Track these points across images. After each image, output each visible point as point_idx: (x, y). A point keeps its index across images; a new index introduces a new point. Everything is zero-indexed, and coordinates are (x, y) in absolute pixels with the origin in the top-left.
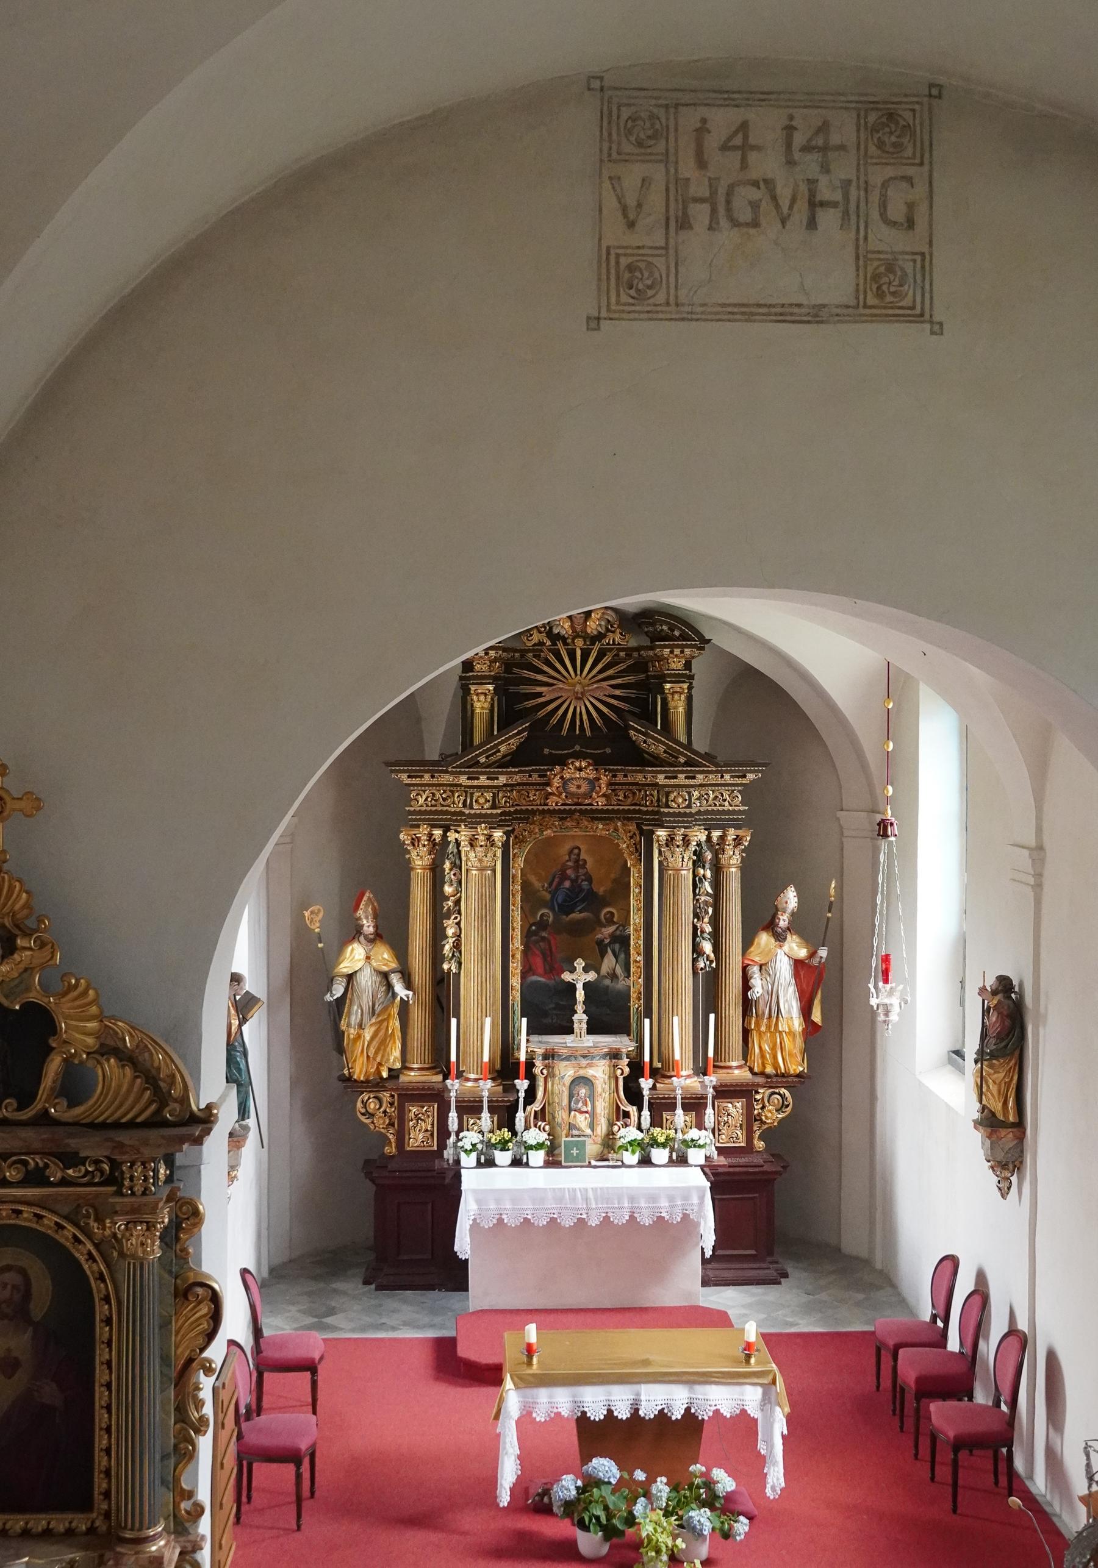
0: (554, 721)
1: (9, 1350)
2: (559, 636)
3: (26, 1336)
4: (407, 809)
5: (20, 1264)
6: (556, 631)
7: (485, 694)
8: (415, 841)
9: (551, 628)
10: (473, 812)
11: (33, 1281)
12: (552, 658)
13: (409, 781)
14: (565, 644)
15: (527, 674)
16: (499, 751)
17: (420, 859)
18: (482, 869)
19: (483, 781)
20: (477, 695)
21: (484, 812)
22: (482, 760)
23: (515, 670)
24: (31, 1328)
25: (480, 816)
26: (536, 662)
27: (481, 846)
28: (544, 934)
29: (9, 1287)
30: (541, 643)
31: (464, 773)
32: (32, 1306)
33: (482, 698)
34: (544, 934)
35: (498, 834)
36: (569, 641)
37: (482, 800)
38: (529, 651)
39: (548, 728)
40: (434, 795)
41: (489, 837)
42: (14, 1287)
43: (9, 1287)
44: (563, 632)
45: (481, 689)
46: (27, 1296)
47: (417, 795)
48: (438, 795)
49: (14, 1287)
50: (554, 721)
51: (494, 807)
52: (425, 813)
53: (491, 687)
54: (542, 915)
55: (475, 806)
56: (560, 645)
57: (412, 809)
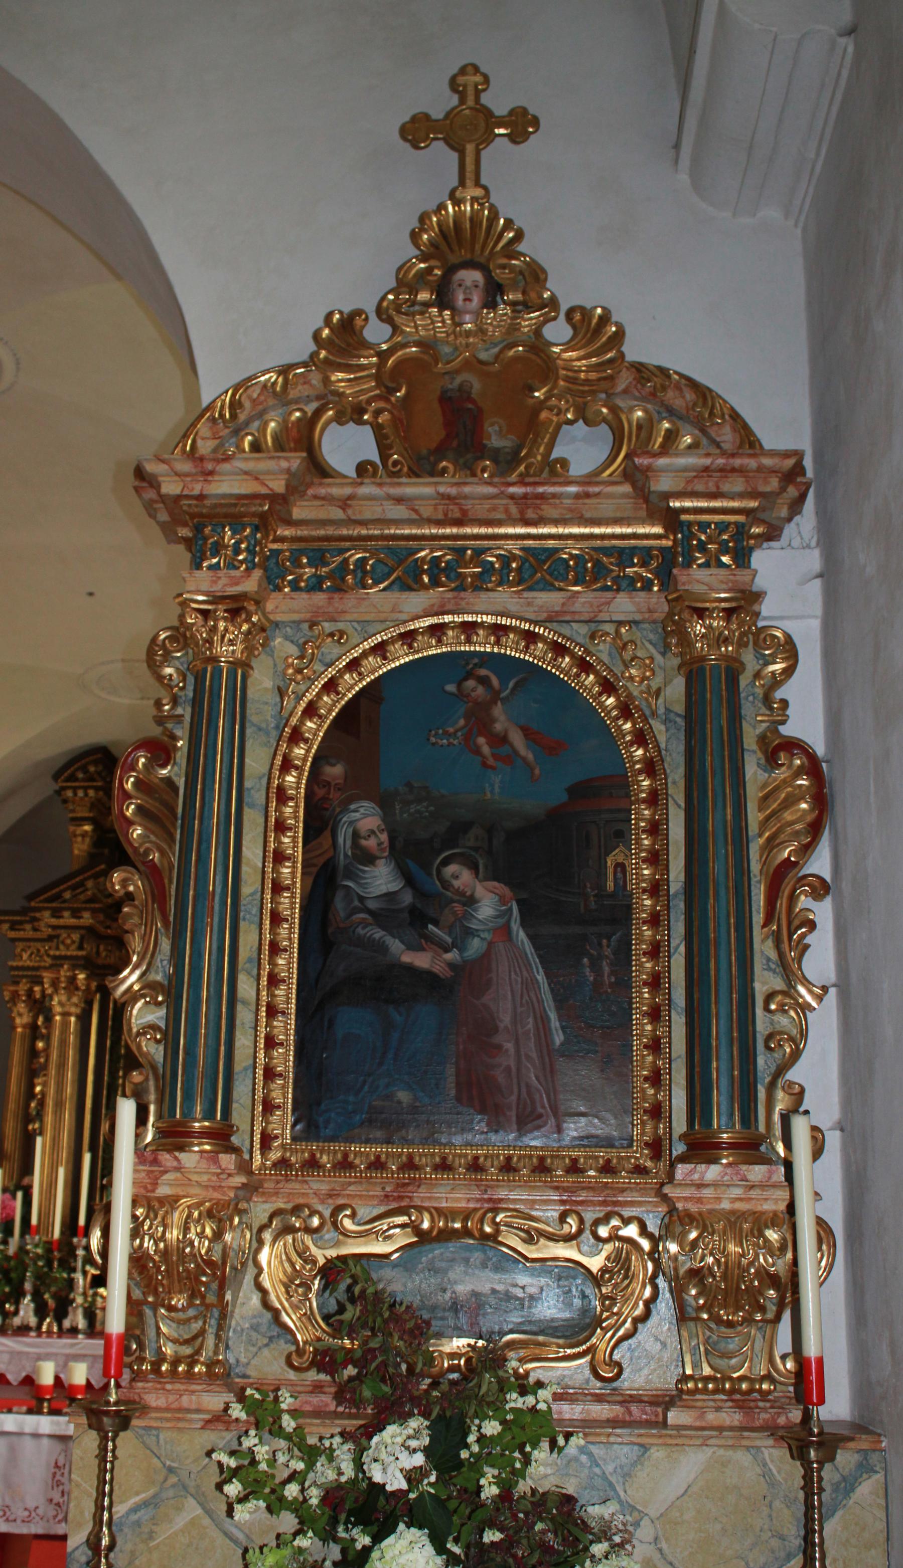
4: (10, 963)
8: (15, 996)
10: (57, 953)
13: (12, 934)
17: (22, 1017)
18: (65, 1015)
19: (67, 919)
21: (69, 953)
25: (66, 958)
33: (79, 839)
40: (38, 950)
41: (72, 980)
47: (23, 950)
48: (42, 951)
51: (81, 948)
52: (28, 968)
53: (87, 828)
55: (62, 947)
57: (15, 964)
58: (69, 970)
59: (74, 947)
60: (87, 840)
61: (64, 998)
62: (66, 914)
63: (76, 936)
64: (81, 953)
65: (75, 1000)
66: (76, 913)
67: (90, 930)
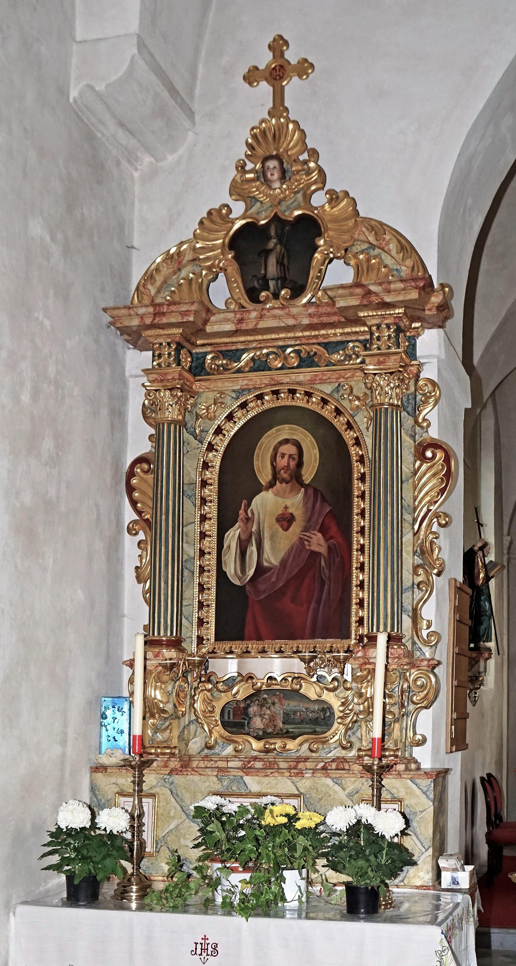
1: (286, 508)
3: (300, 495)
5: (295, 437)
24: (303, 489)
29: (286, 457)
42: (290, 456)
43: (286, 457)
46: (300, 464)
49: (290, 456)
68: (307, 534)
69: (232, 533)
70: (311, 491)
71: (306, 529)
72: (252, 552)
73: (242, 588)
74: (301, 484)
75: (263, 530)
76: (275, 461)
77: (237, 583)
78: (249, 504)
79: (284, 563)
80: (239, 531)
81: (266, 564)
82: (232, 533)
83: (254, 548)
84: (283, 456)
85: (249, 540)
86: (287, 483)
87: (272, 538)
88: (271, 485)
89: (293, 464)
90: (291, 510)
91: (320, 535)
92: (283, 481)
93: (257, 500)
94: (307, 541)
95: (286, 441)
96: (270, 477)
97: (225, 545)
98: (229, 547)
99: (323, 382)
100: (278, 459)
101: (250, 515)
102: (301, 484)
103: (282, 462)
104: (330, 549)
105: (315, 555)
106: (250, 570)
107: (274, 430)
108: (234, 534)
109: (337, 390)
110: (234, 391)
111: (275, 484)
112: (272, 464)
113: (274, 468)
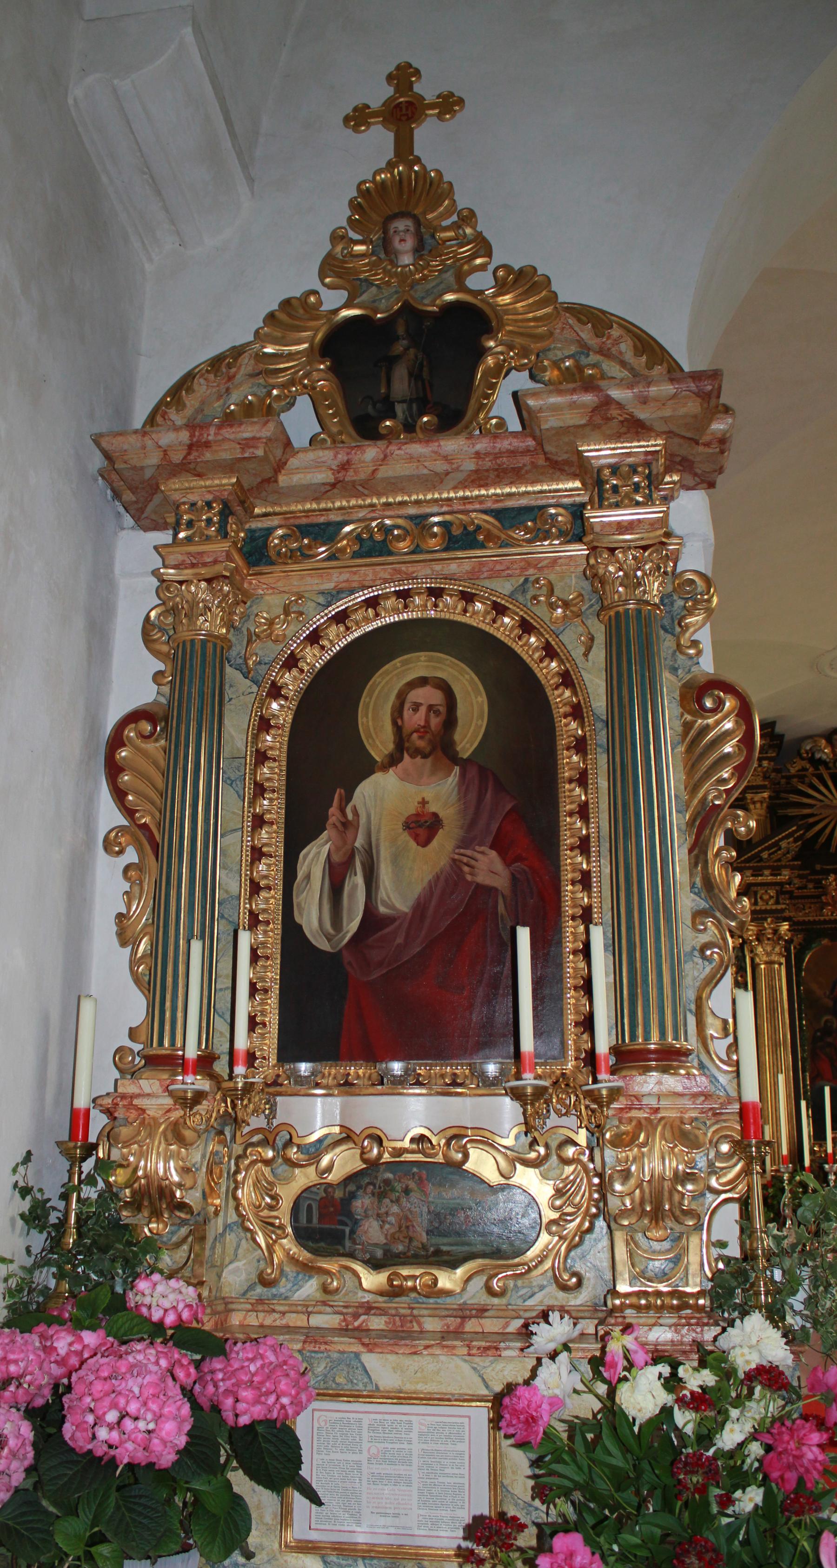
0: (822, 839)
1: (424, 802)
2: (821, 762)
3: (450, 779)
5: (439, 674)
6: (818, 756)
7: (761, 802)
9: (813, 754)
11: (458, 701)
12: (816, 782)
14: (827, 768)
15: (794, 798)
16: (780, 849)
18: (770, 963)
19: (767, 877)
20: (754, 803)
21: (768, 908)
22: (765, 855)
23: (783, 795)
24: (457, 769)
25: (766, 912)
26: (801, 787)
27: (769, 939)
28: (829, 1040)
30: (804, 769)
31: (749, 868)
32: (457, 737)
33: (758, 805)
34: (829, 1040)
35: (785, 927)
36: (831, 765)
37: (766, 897)
38: (794, 776)
39: (817, 847)
41: (775, 931)
42: (430, 708)
43: (423, 710)
44: (824, 757)
45: (757, 797)
46: (450, 722)
49: (430, 708)
50: (822, 839)
54: (826, 1021)
56: (822, 770)
58: (772, 922)
59: (772, 902)
60: (765, 805)
61: (769, 949)
62: (767, 872)
63: (772, 893)
64: (779, 907)
65: (777, 949)
66: (776, 871)
67: (781, 884)
68: (468, 852)
69: (314, 850)
70: (473, 772)
71: (465, 843)
72: (355, 887)
73: (335, 957)
74: (454, 758)
75: (378, 846)
76: (401, 715)
77: (323, 945)
78: (349, 797)
79: (420, 908)
80: (327, 847)
81: (382, 910)
82: (314, 850)
83: (359, 879)
84: (416, 707)
85: (348, 863)
86: (425, 756)
87: (395, 860)
88: (393, 761)
89: (435, 721)
90: (433, 808)
91: (493, 854)
92: (416, 753)
93: (365, 791)
94: (467, 865)
95: (423, 681)
96: (391, 746)
97: (300, 874)
98: (308, 877)
99: (495, 574)
100: (407, 713)
101: (350, 816)
102: (454, 758)
103: (414, 719)
104: (514, 879)
105: (485, 891)
106: (351, 920)
107: (397, 662)
108: (319, 853)
109: (523, 588)
110: (322, 593)
111: (401, 759)
112: (394, 723)
113: (398, 729)
